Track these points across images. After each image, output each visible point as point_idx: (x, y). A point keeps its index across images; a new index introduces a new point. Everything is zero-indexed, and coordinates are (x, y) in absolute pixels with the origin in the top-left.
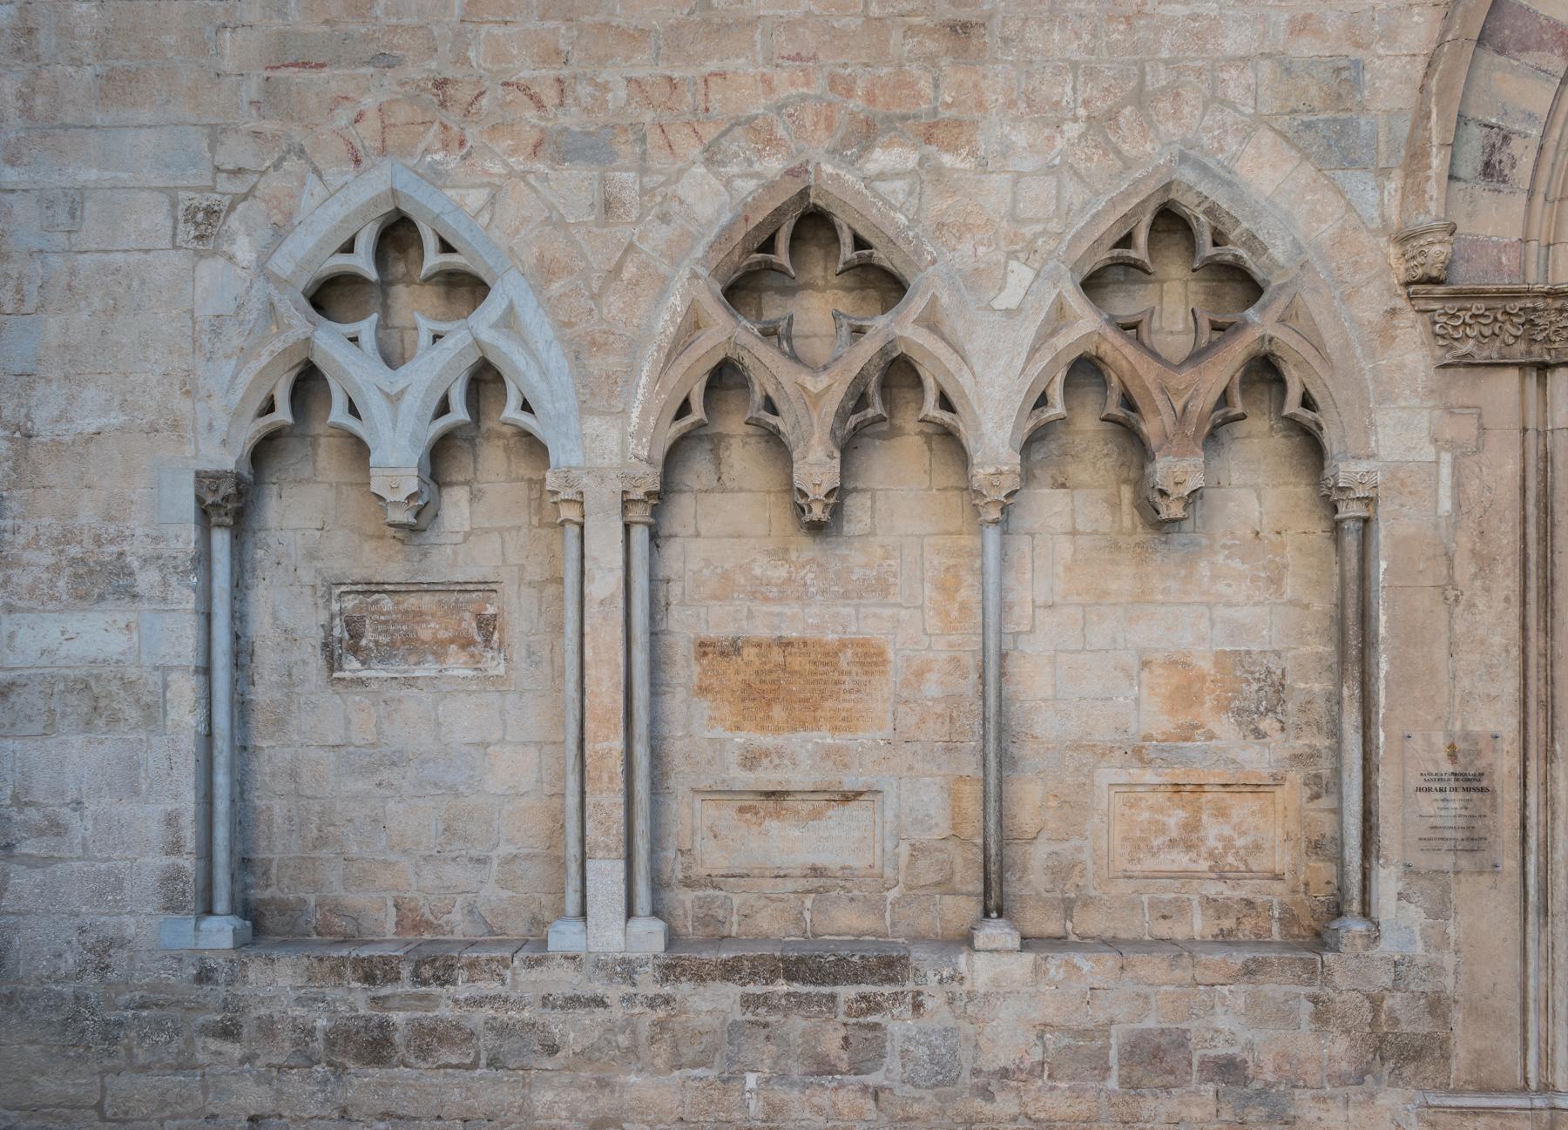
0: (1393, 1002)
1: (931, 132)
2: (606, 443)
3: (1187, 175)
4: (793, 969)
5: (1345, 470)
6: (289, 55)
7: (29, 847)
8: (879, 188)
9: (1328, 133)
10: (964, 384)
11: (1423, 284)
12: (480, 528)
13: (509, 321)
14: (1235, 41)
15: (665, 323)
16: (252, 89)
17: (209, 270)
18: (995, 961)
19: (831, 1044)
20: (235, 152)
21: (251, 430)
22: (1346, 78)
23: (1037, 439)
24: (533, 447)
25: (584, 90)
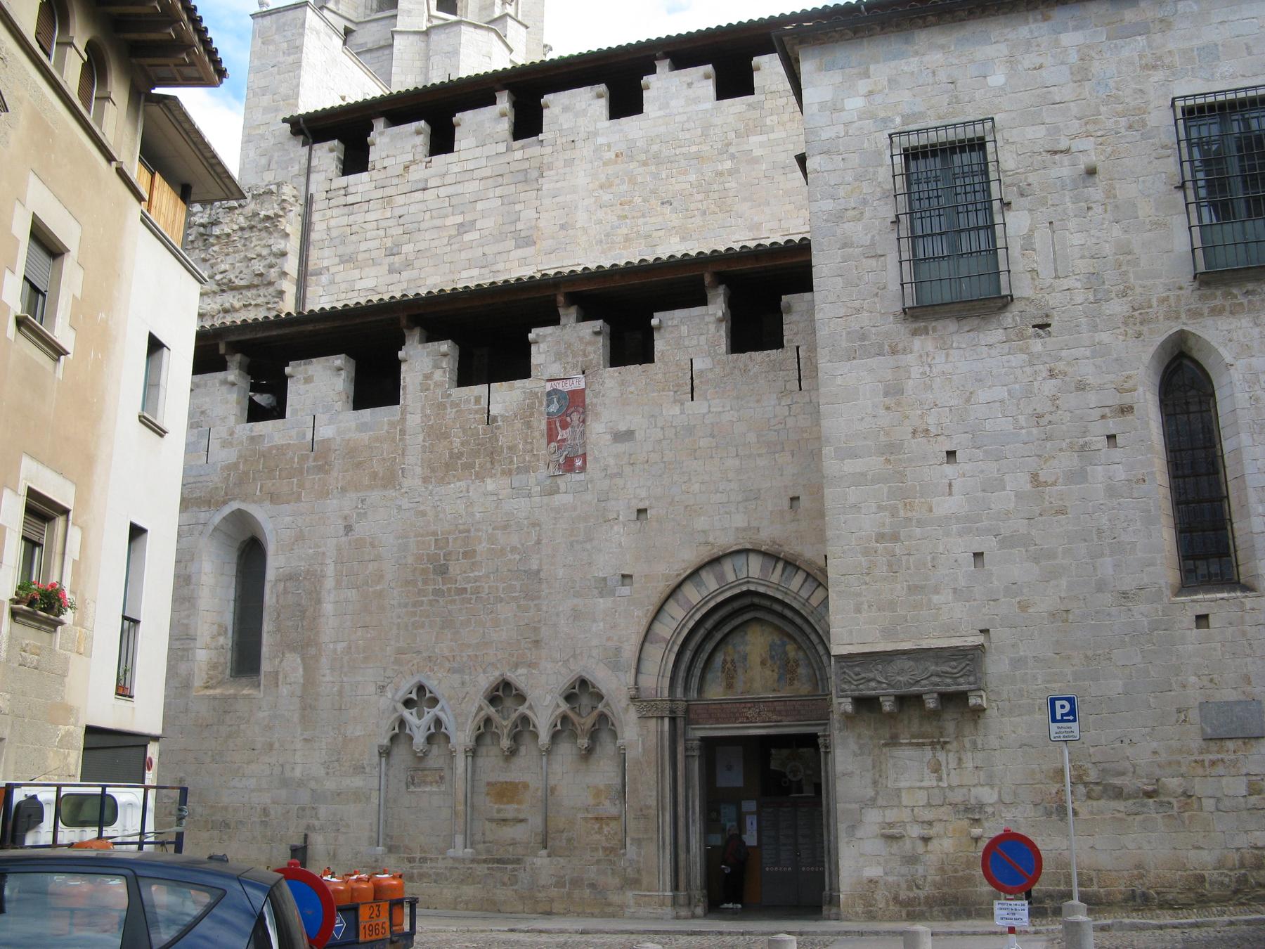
0: (629, 870)
1: (531, 665)
2: (462, 737)
3: (584, 674)
4: (499, 861)
5: (619, 742)
6: (400, 651)
7: (343, 830)
8: (519, 678)
9: (614, 664)
10: (537, 722)
11: (633, 699)
12: (436, 758)
13: (442, 709)
14: (595, 642)
15: (474, 710)
16: (392, 659)
17: (383, 699)
18: (541, 860)
19: (506, 879)
20: (389, 673)
21: (391, 734)
22: (618, 650)
23: (555, 737)
24: (447, 738)
25: (458, 658)
